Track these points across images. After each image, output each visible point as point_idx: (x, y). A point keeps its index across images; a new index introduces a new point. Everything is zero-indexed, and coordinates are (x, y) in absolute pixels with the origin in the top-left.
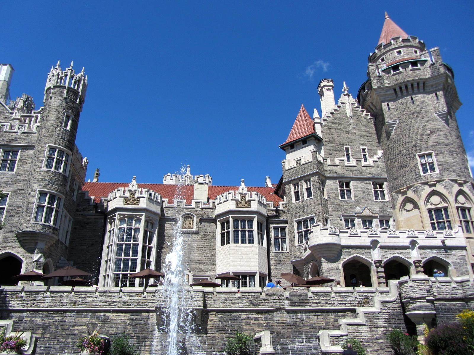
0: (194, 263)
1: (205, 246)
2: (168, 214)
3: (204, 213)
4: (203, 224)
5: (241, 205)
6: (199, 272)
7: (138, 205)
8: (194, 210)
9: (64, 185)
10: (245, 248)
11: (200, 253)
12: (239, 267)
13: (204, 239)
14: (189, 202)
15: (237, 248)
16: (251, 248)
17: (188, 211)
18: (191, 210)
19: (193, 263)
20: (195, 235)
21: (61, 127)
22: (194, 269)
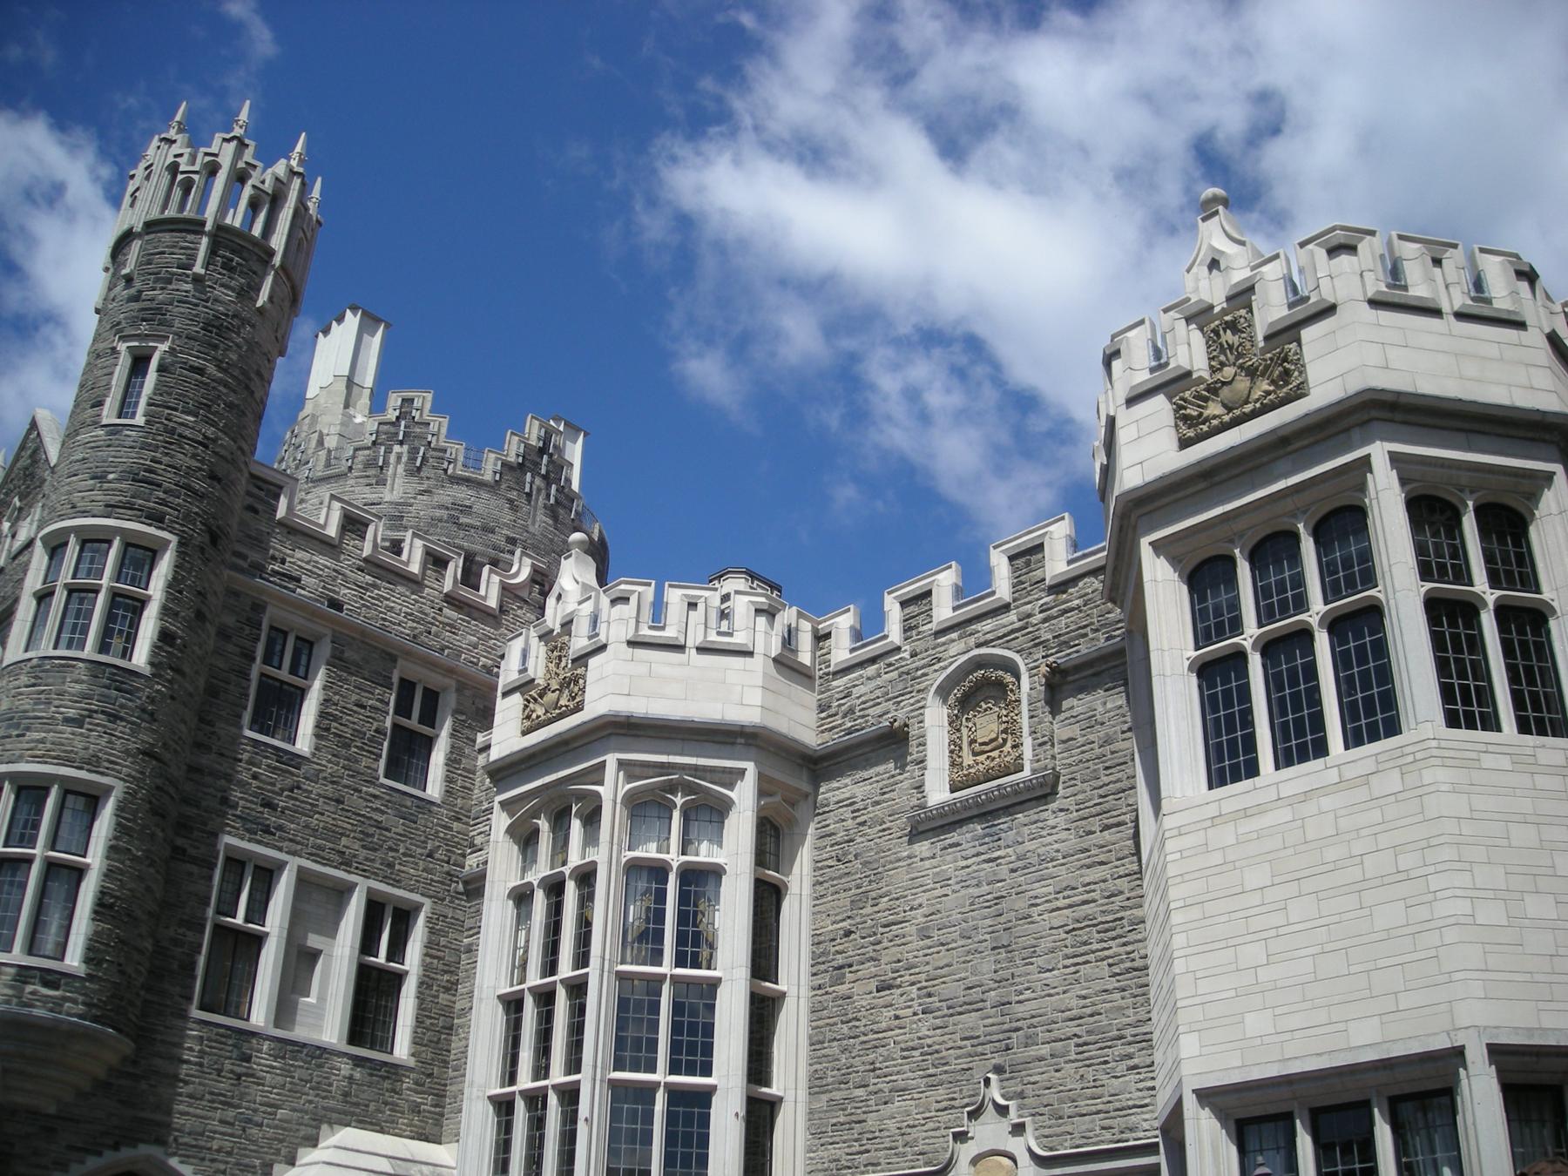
0: (1045, 1050)
1: (1111, 886)
2: (851, 711)
3: (1074, 616)
4: (1075, 705)
5: (1214, 409)
6: (1082, 1124)
7: (579, 708)
8: (1012, 617)
9: (100, 719)
10: (1310, 808)
11: (1078, 959)
12: (1257, 1023)
13: (1095, 824)
14: (975, 579)
15: (1226, 834)
16: (1361, 794)
17: (972, 641)
18: (987, 625)
19: (1034, 1051)
20: (1032, 814)
21: (96, 424)
22: (1049, 1096)
